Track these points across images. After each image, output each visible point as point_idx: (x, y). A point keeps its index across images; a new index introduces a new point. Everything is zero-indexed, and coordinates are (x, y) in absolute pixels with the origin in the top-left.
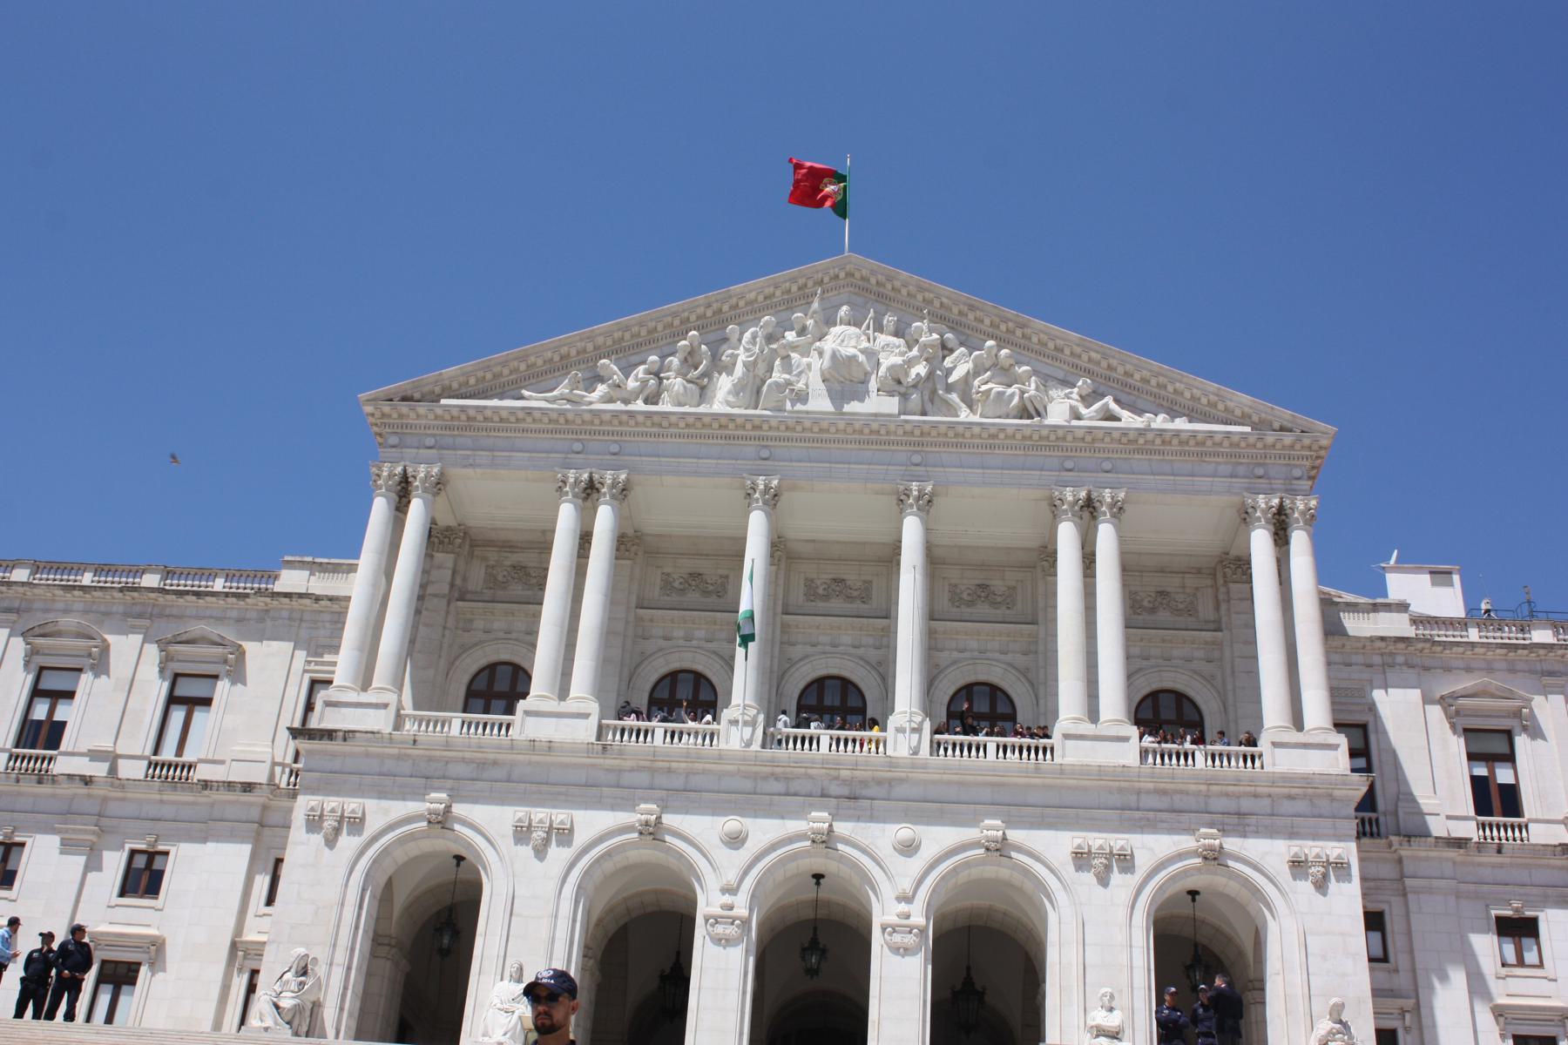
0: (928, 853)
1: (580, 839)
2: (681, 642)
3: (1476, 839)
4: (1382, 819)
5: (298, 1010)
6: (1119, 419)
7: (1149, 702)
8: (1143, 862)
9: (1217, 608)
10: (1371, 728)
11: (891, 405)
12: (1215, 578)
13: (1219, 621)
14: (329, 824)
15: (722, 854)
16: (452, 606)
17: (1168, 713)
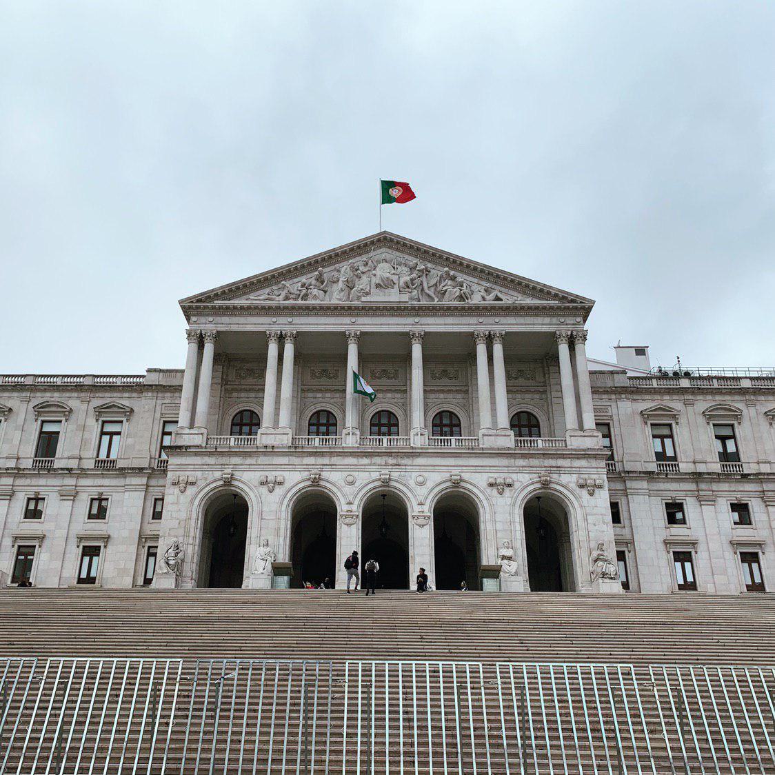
0: (430, 484)
1: (287, 485)
2: (321, 399)
3: (657, 471)
4: (616, 464)
5: (174, 565)
6: (502, 300)
7: (516, 417)
8: (517, 485)
9: (544, 376)
10: (611, 425)
11: (405, 297)
12: (542, 363)
13: (545, 382)
14: (182, 485)
15: (348, 490)
16: (223, 387)
17: (524, 422)
